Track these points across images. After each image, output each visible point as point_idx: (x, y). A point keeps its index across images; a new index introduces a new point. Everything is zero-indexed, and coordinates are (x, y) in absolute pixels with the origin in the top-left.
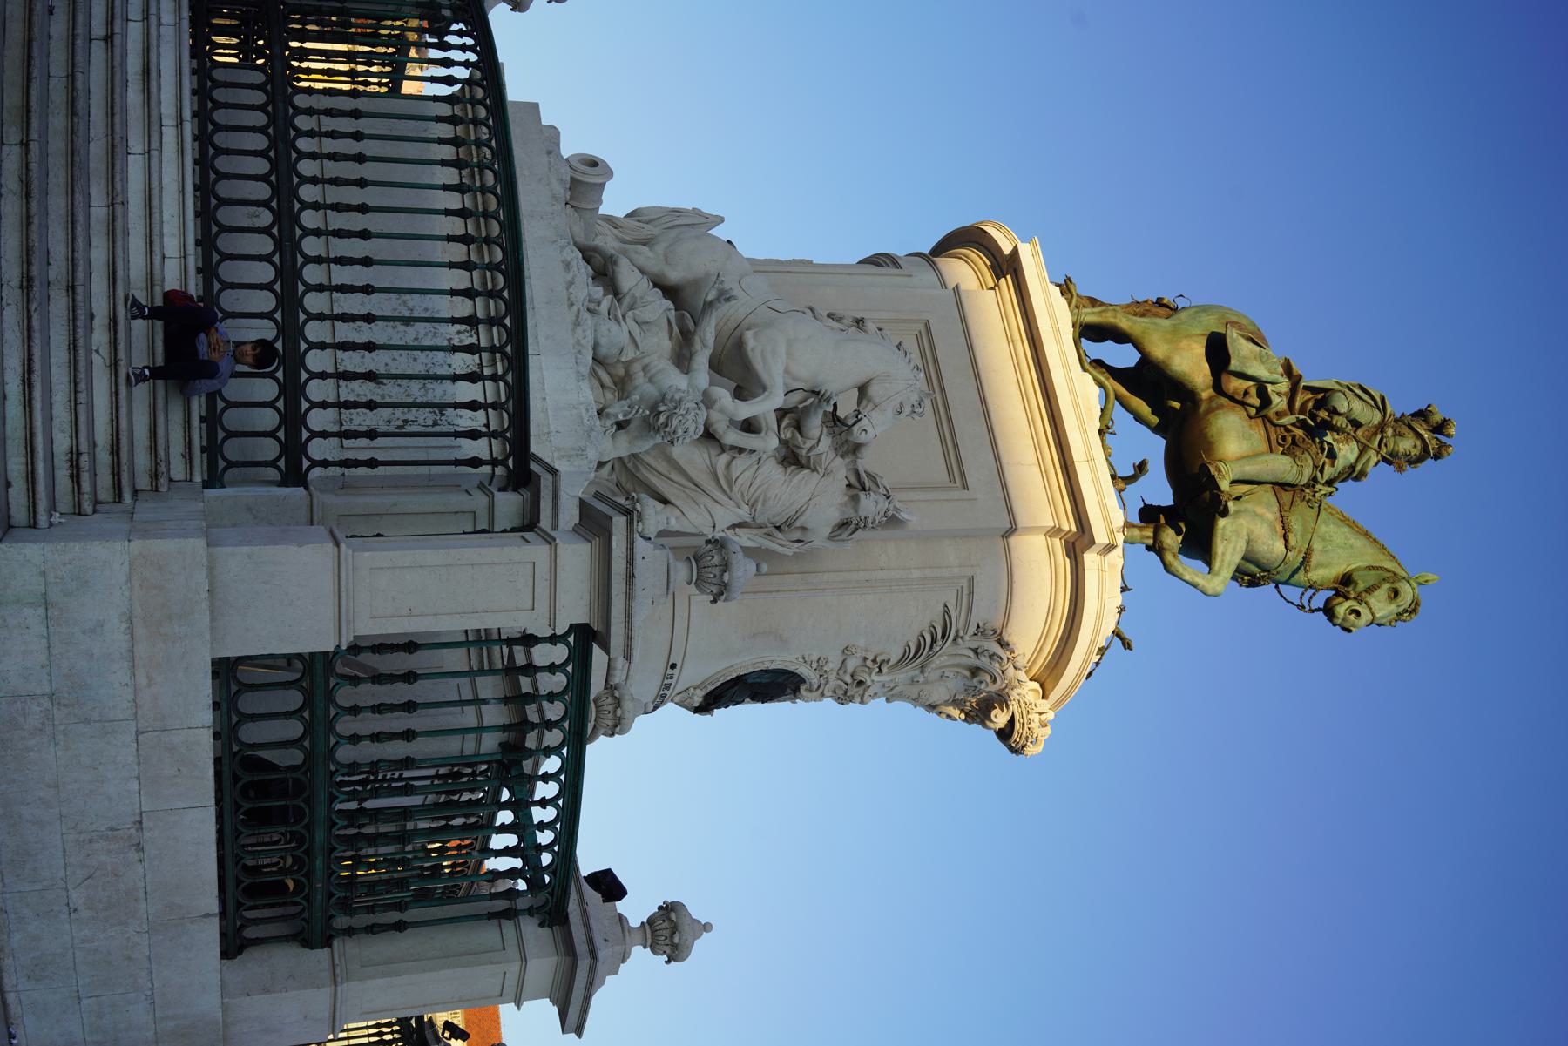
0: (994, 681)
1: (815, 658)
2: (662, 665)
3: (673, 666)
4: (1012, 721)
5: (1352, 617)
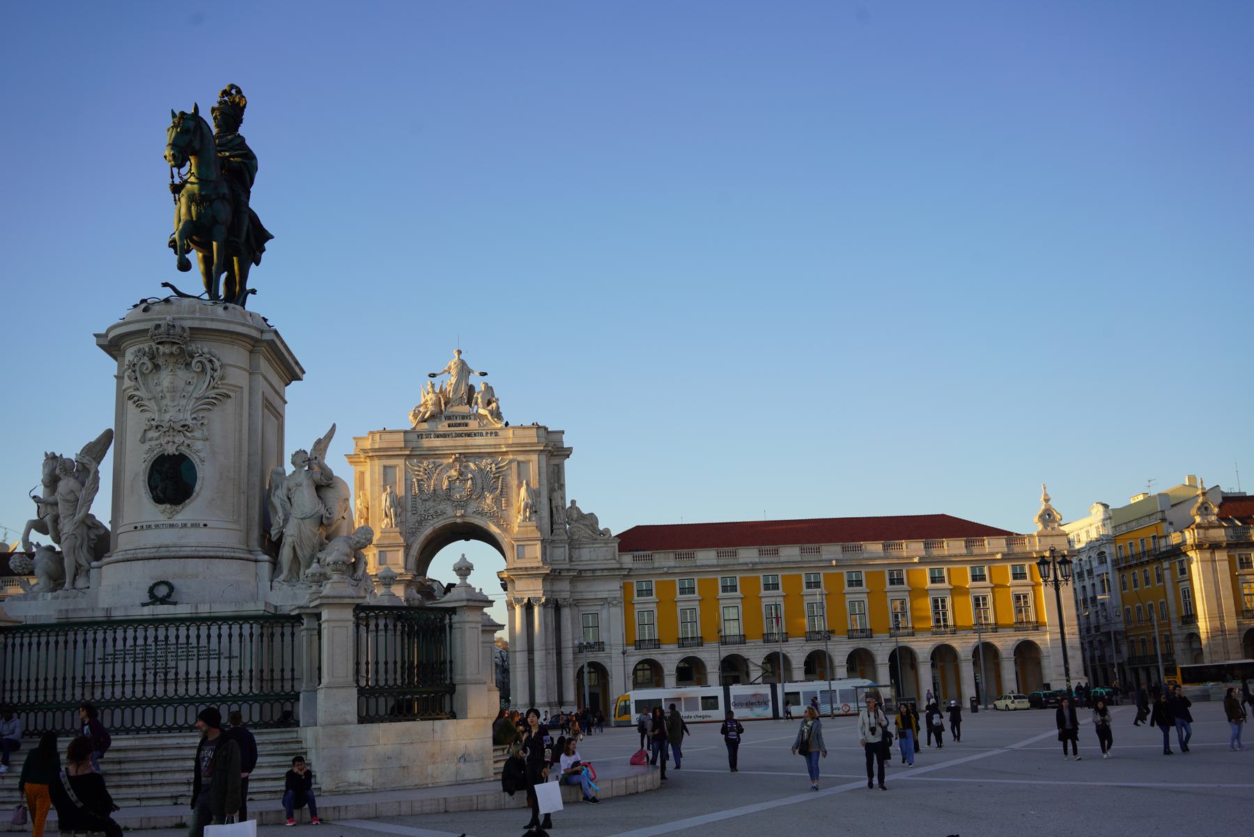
2: (136, 533)
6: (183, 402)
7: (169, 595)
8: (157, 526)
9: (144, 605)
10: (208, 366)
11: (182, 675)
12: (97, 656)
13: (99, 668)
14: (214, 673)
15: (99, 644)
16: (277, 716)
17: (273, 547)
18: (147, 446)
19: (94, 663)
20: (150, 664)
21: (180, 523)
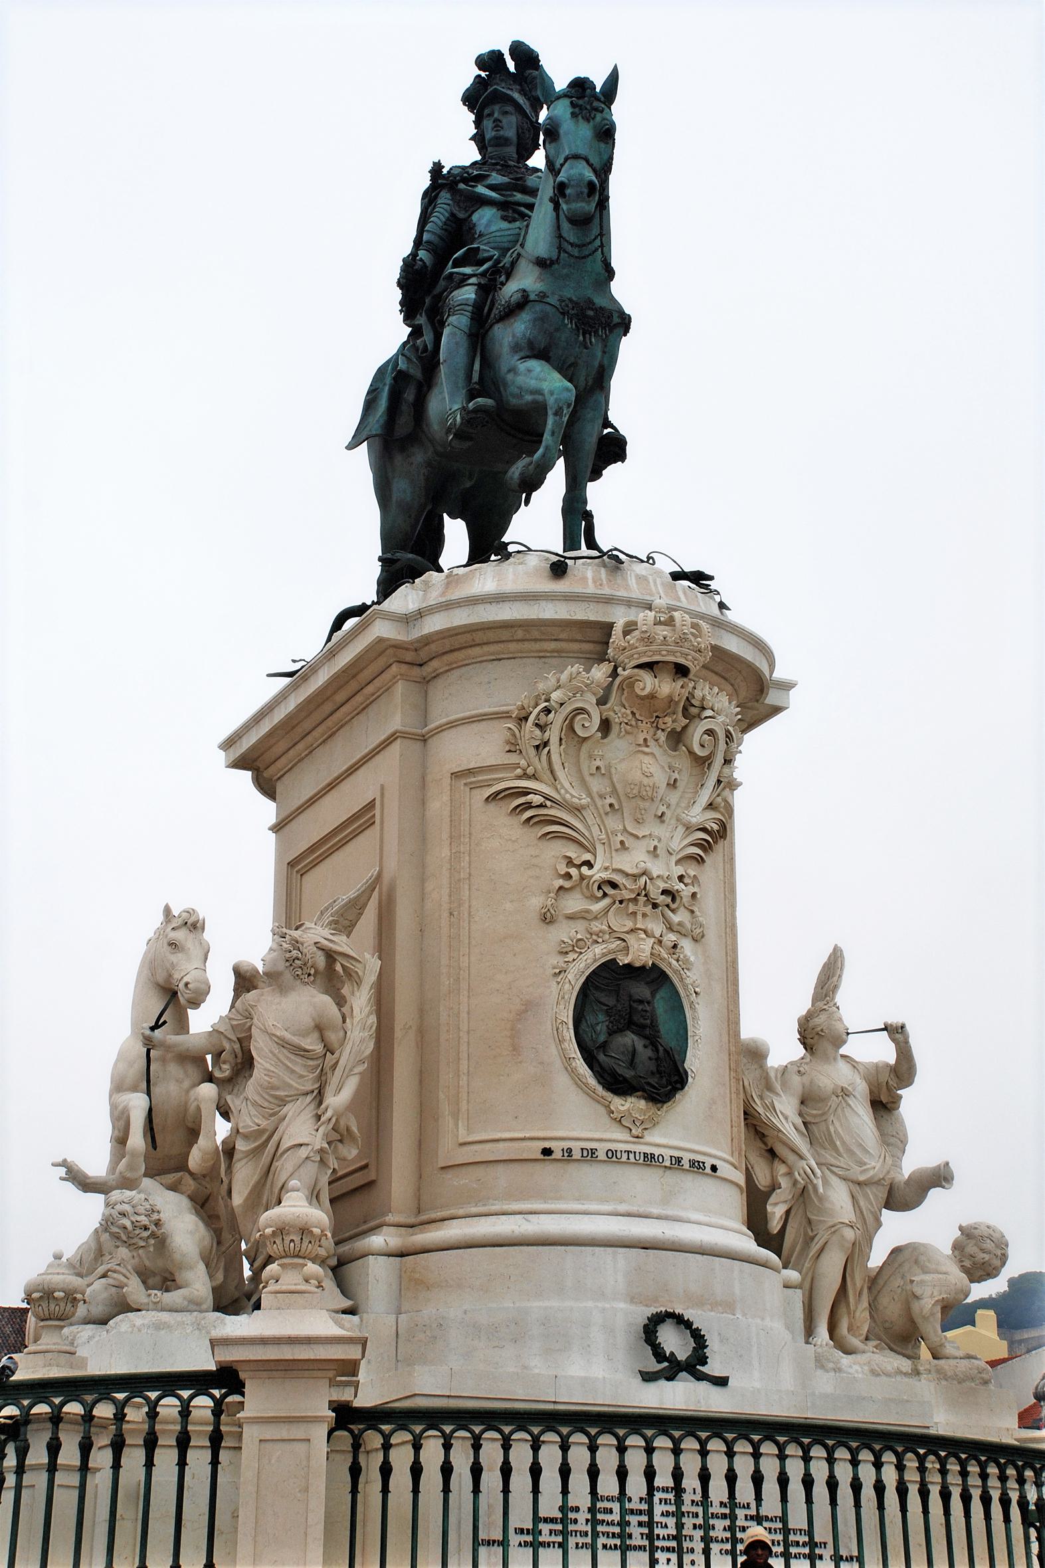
0: (582, 710)
1: (559, 961)
3: (547, 1152)
4: (649, 666)
5: (568, 191)
6: (659, 830)
7: (699, 1356)
8: (612, 1154)
9: (648, 1377)
12: (514, 1523)
15: (521, 1481)
18: (566, 932)
19: (504, 1543)
21: (667, 1153)
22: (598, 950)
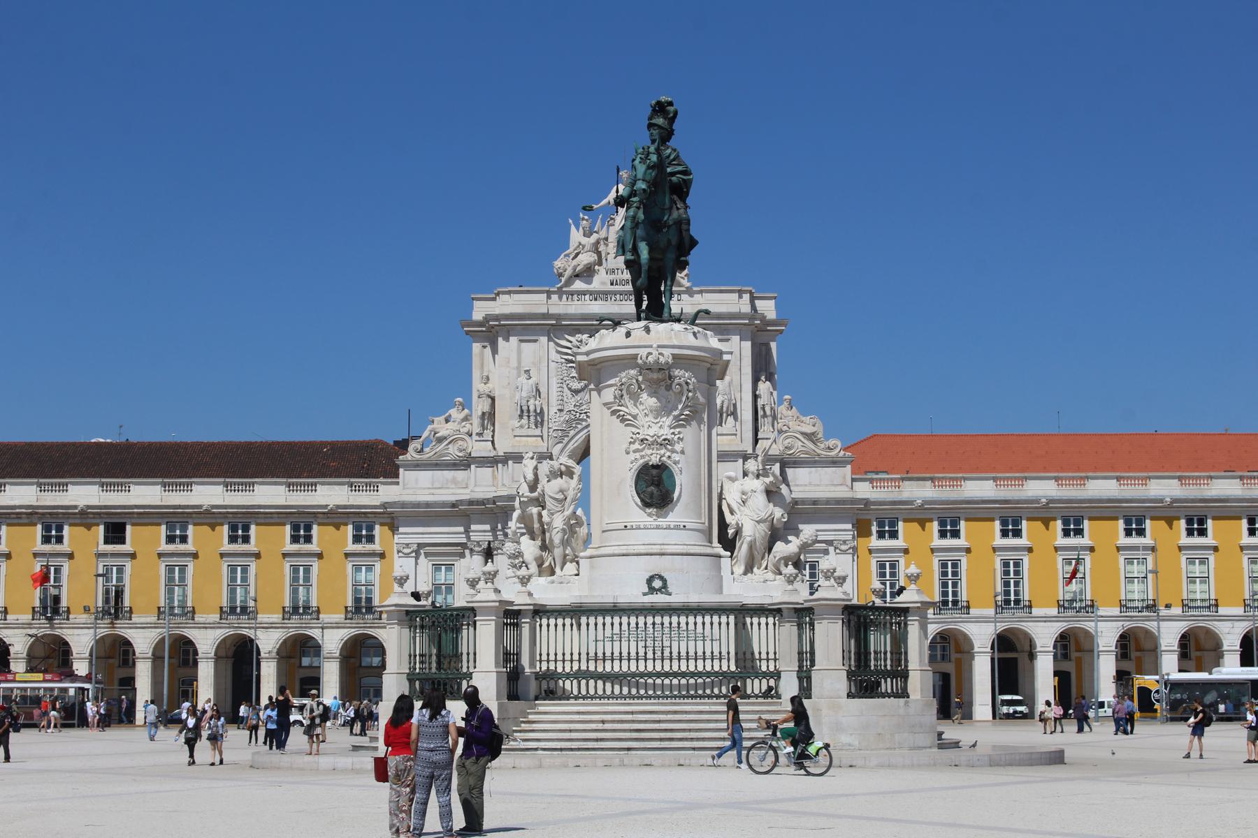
7: (665, 586)
9: (645, 594)
10: (685, 387)
11: (675, 654)
13: (608, 645)
14: (700, 653)
15: (608, 626)
16: (764, 688)
17: (729, 544)
18: (632, 456)
20: (650, 643)
22: (642, 461)
